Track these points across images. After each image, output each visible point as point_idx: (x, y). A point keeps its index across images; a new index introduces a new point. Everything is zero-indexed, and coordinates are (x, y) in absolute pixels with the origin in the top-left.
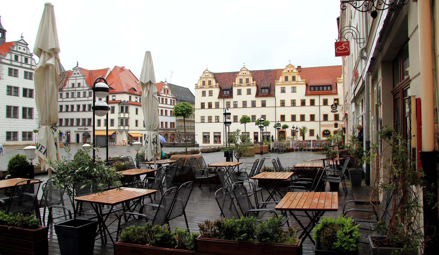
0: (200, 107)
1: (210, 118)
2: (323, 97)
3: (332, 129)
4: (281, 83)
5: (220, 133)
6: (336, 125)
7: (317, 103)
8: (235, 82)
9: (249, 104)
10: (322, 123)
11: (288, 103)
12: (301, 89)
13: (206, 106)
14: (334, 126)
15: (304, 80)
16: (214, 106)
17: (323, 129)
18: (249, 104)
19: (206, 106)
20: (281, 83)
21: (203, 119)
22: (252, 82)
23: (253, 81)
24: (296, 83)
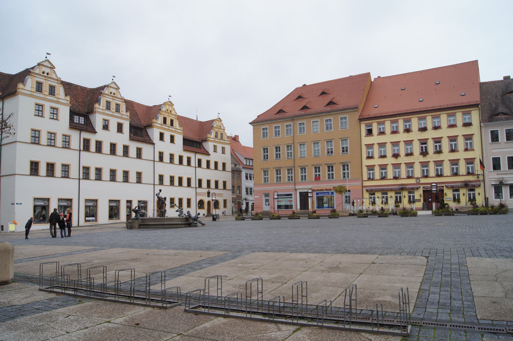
0: (29, 139)
1: (51, 167)
2: (199, 156)
3: (206, 199)
4: (160, 126)
5: (71, 200)
6: (209, 193)
7: (193, 163)
8: (100, 105)
9: (120, 150)
10: (199, 190)
11: (166, 158)
12: (179, 139)
13: (44, 140)
14: (207, 194)
15: (182, 128)
16: (59, 142)
17: (199, 198)
18: (120, 150)
19: (44, 140)
20: (160, 126)
21: (34, 167)
22: (124, 113)
23: (127, 111)
24: (174, 130)
